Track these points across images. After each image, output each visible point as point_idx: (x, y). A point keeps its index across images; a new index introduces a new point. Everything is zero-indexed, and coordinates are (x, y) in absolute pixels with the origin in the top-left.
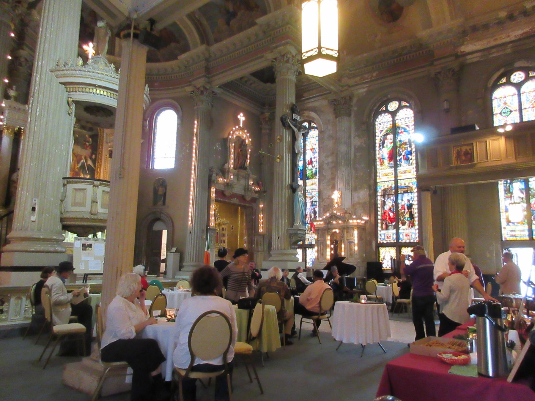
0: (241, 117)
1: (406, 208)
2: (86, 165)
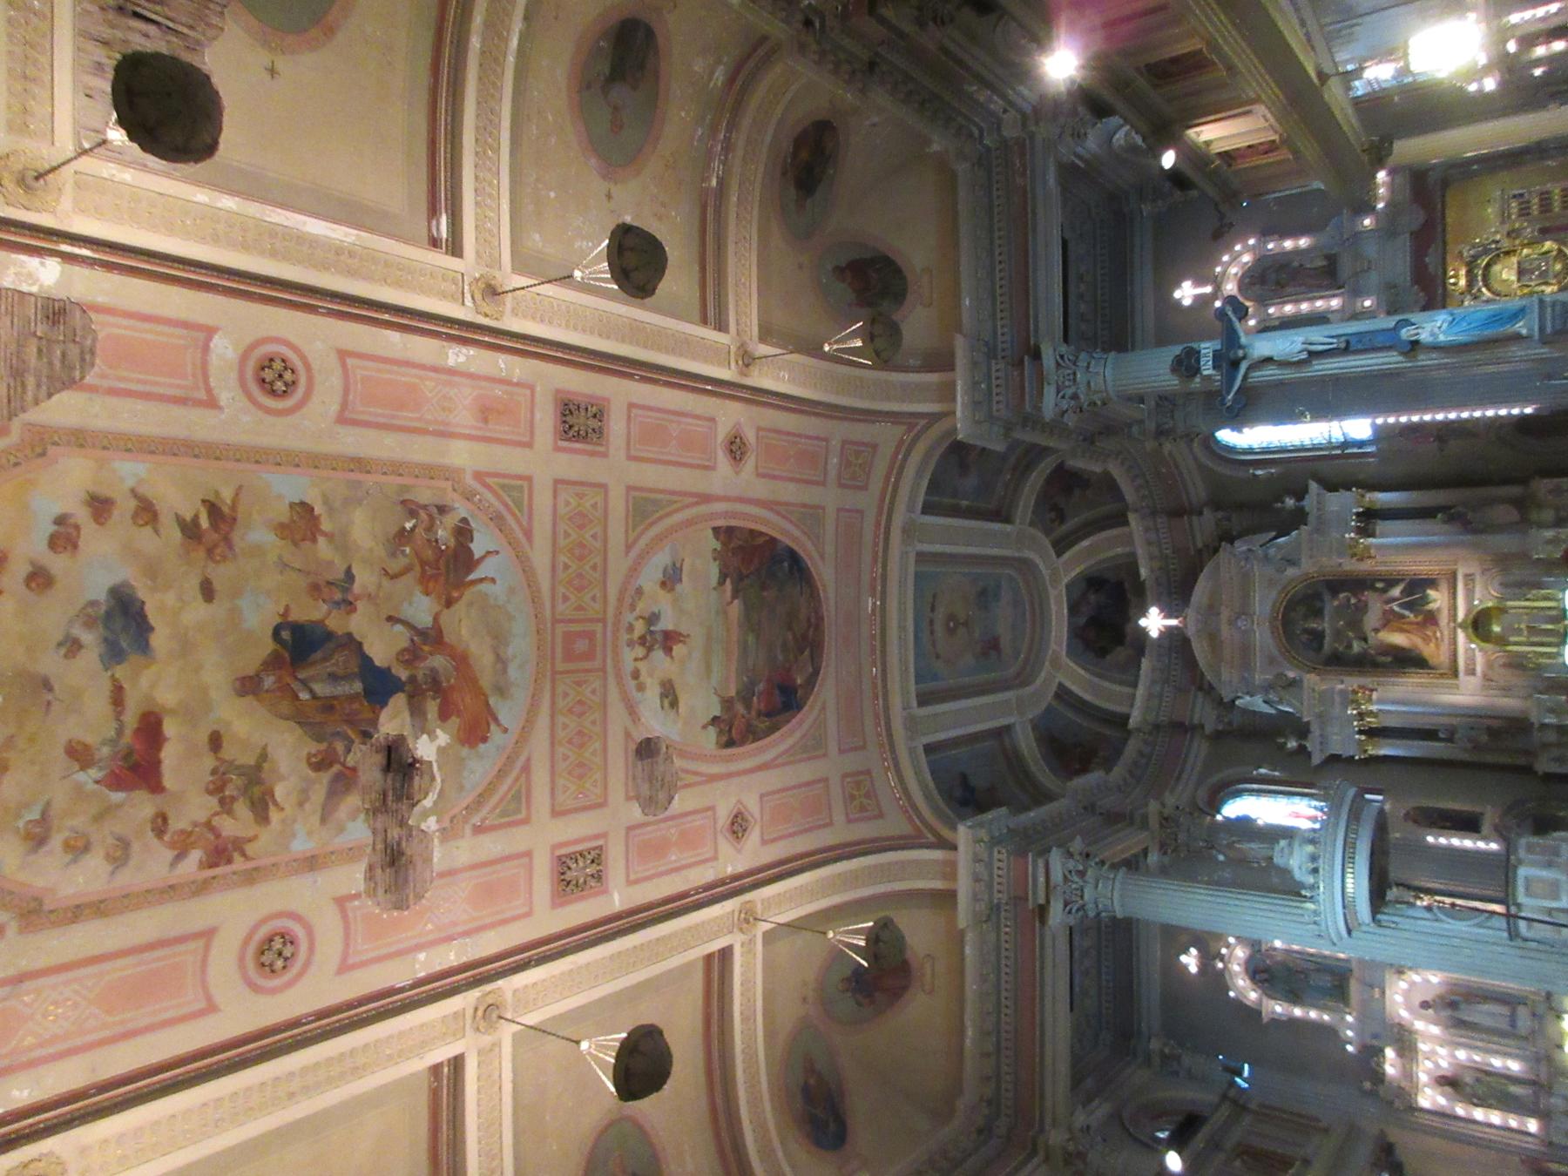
0: (1186, 293)
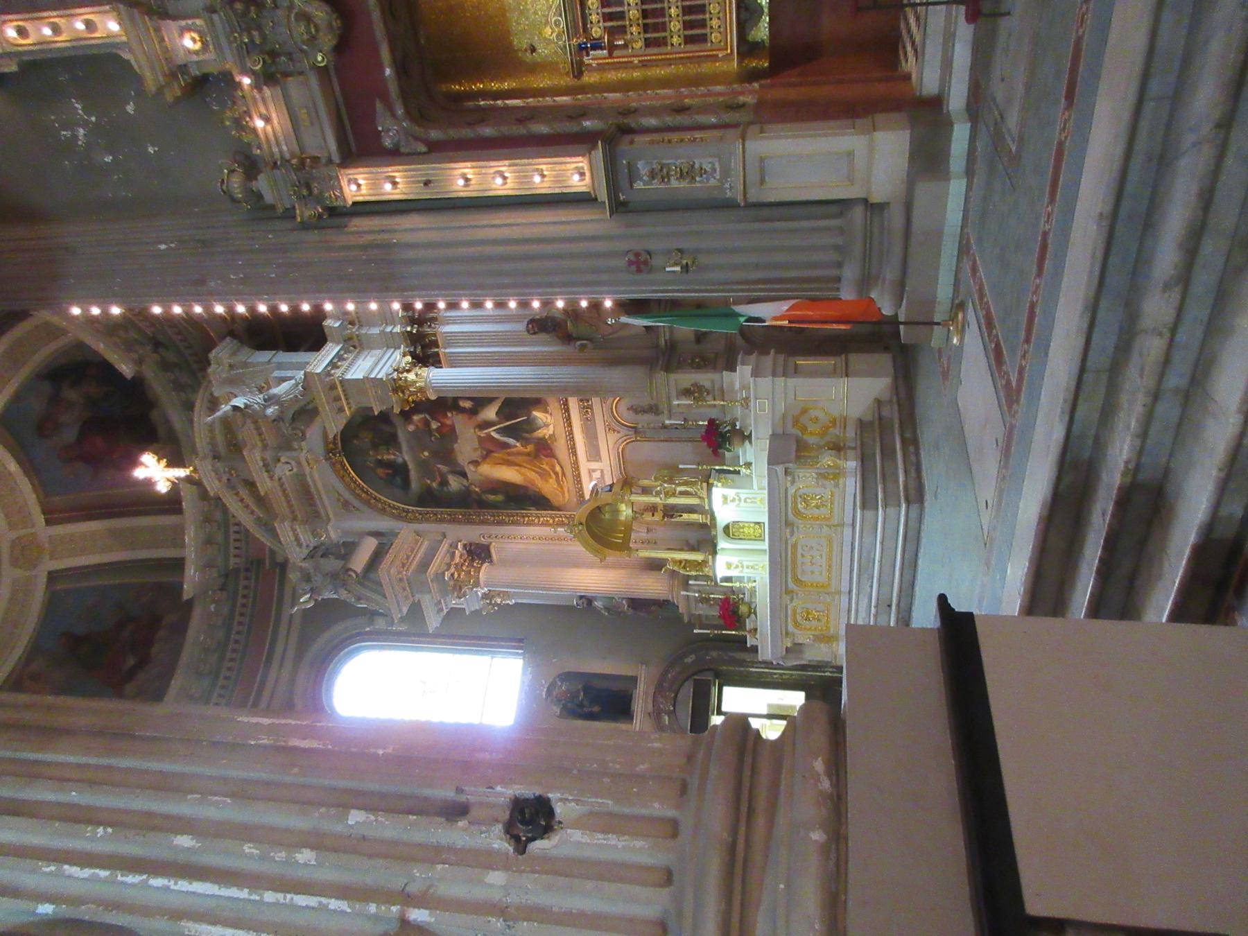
2: (502, 425)
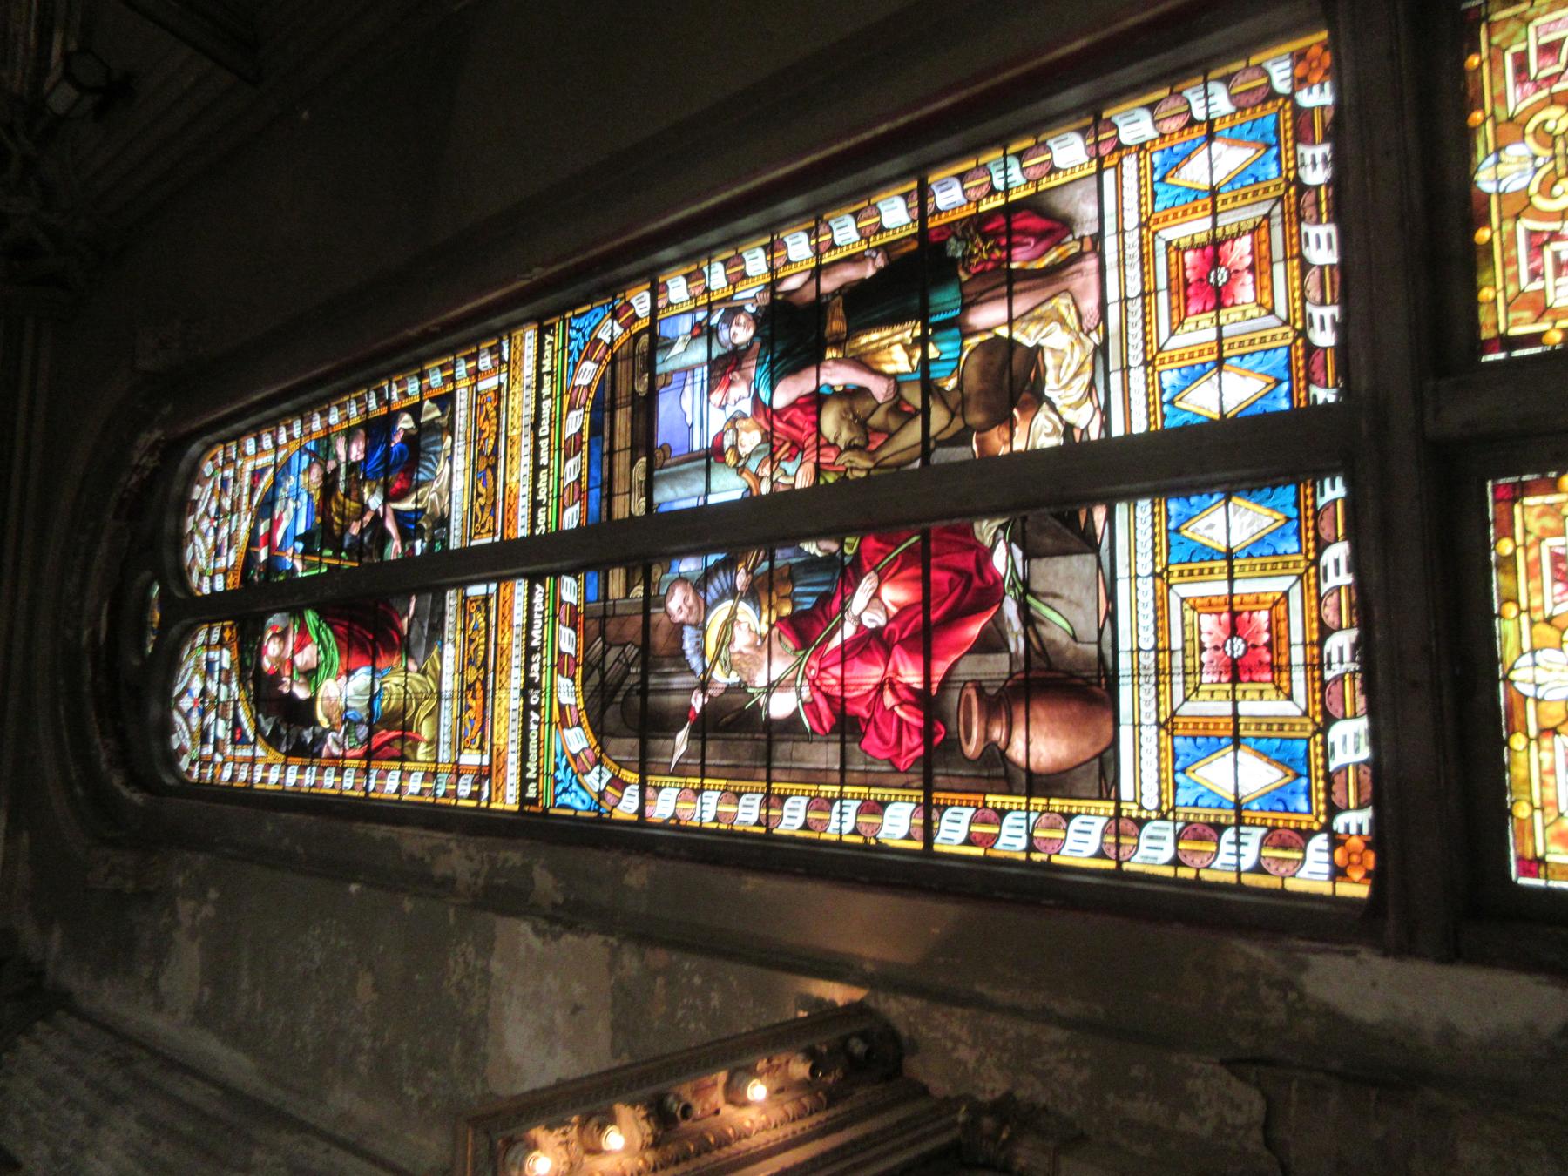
1: (804, 384)
